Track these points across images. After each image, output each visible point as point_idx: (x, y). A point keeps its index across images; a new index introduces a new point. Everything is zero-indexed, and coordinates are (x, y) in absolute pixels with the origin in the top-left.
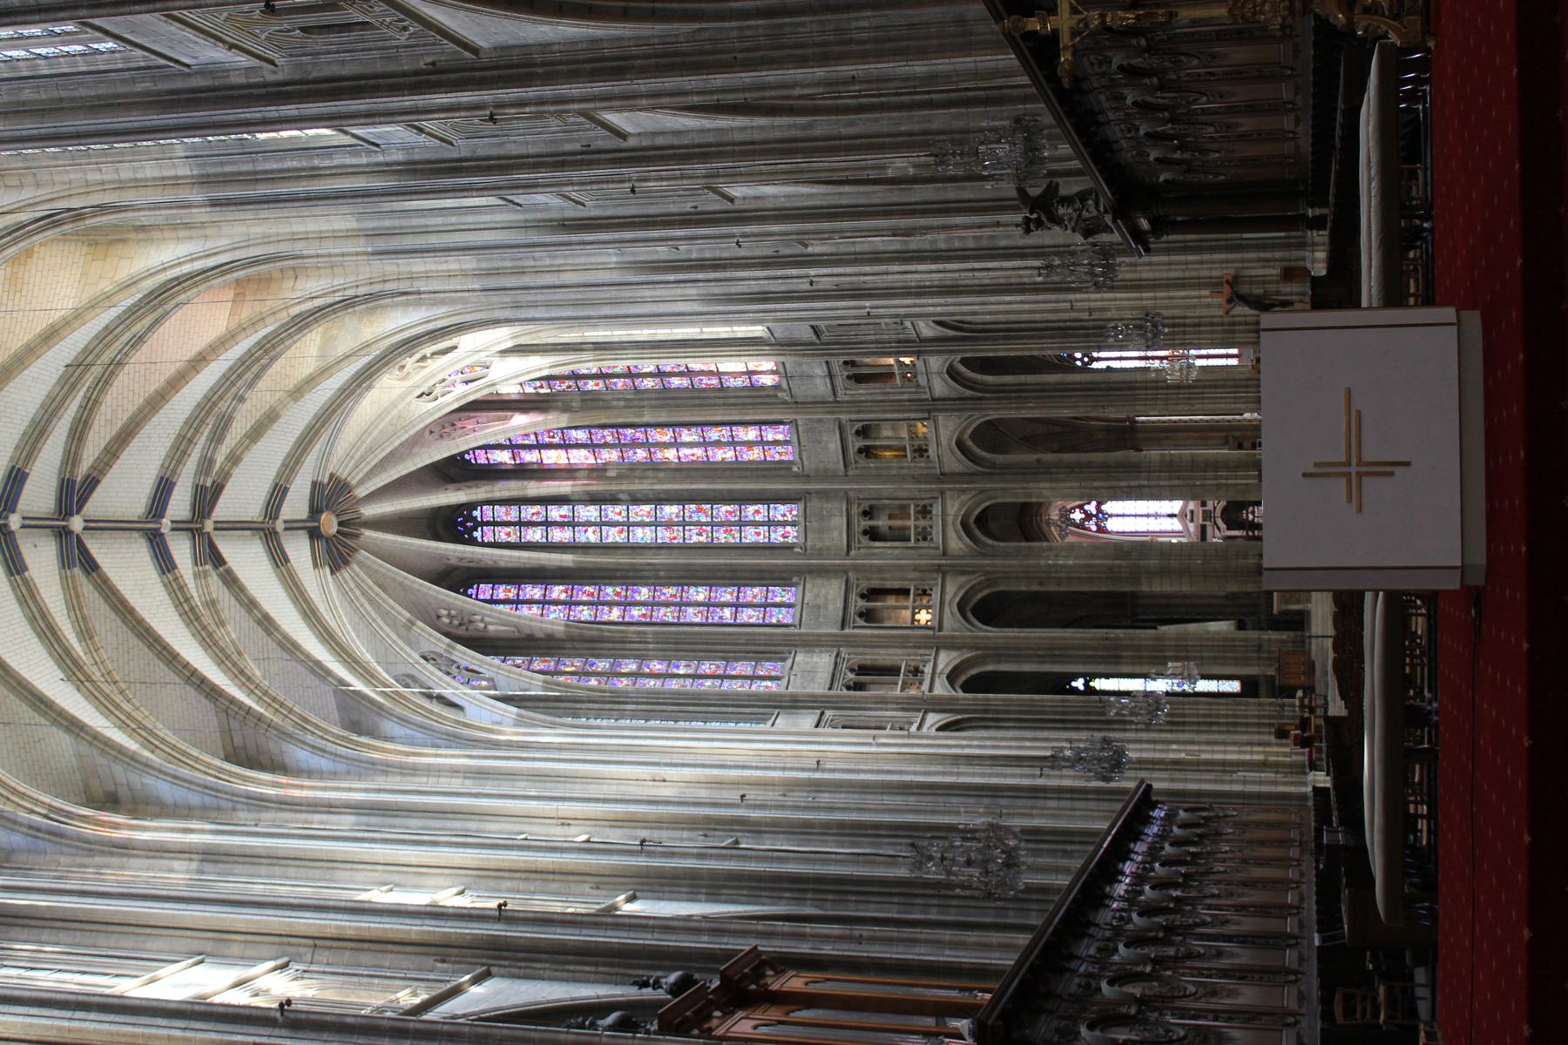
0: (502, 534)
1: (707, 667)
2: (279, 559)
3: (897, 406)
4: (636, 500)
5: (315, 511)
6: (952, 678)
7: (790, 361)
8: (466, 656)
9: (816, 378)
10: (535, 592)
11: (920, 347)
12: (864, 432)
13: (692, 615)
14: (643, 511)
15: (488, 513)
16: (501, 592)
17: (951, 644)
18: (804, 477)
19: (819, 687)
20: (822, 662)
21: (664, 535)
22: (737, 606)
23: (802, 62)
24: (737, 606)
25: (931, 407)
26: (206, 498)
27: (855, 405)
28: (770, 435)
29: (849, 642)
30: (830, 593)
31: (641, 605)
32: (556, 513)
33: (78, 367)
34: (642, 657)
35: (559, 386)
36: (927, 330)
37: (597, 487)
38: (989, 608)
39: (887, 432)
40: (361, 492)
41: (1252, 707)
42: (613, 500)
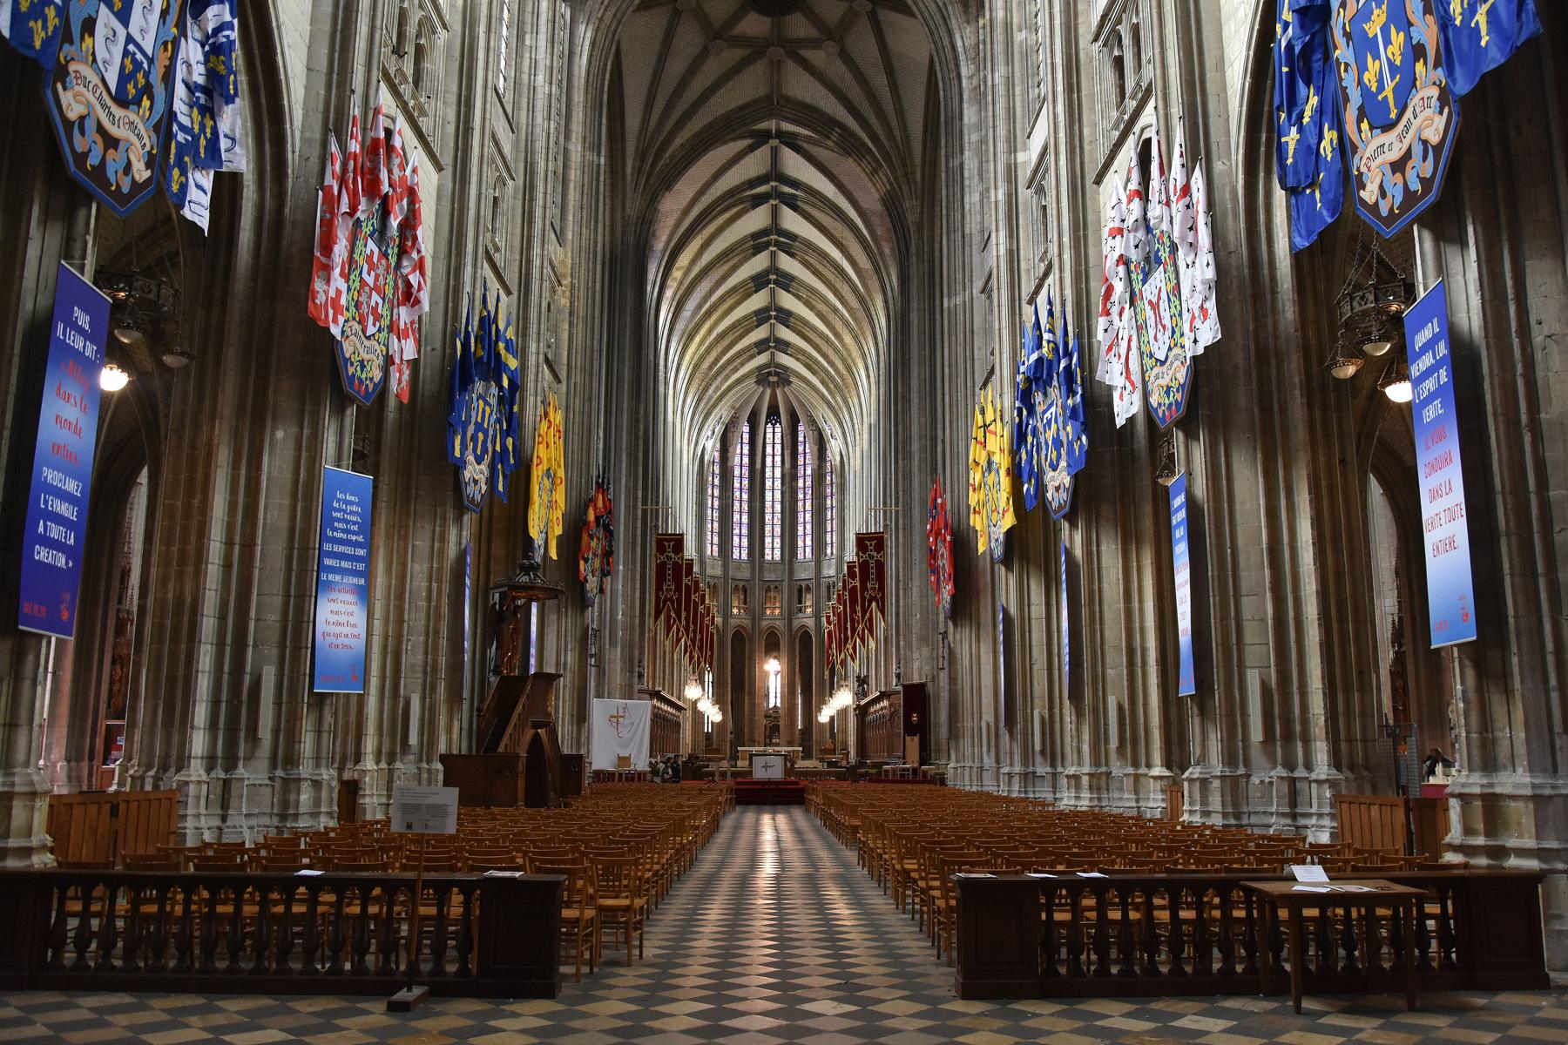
0: (769, 436)
1: (716, 525)
2: (759, 368)
4: (782, 493)
5: (777, 374)
8: (719, 430)
9: (829, 570)
12: (808, 588)
13: (736, 517)
14: (778, 495)
15: (778, 430)
16: (746, 437)
18: (791, 564)
19: (709, 571)
20: (718, 572)
21: (768, 504)
27: (818, 585)
28: (808, 550)
29: (726, 582)
30: (746, 574)
31: (741, 497)
32: (778, 459)
34: (720, 498)
38: (740, 638)
39: (809, 596)
41: (702, 739)
42: (783, 484)
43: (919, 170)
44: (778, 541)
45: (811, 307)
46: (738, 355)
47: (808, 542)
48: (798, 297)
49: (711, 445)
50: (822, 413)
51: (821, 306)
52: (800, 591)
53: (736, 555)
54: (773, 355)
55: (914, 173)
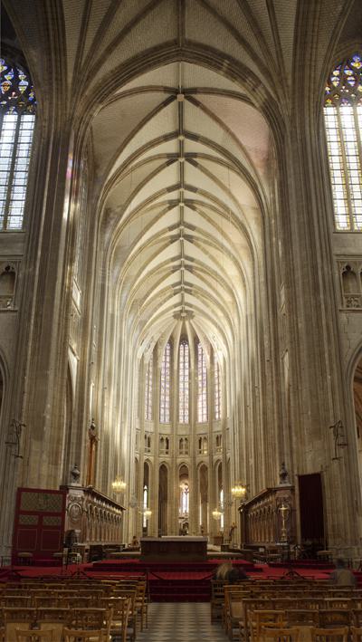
0: (182, 352)
1: (150, 402)
2: (175, 306)
3: (211, 448)
4: (190, 384)
5: (187, 311)
6: (147, 459)
7: (221, 422)
9: (218, 428)
10: (168, 359)
11: (225, 453)
13: (163, 397)
16: (168, 352)
17: (155, 460)
18: (195, 424)
21: (181, 390)
22: (164, 408)
23: (265, 449)
24: (164, 408)
25: (211, 455)
26: (189, 292)
27: (211, 438)
28: (205, 417)
29: (156, 435)
30: (167, 431)
32: (187, 364)
33: (216, 274)
35: (216, 366)
36: (228, 455)
37: (193, 375)
39: (205, 444)
40: (191, 321)
42: (190, 378)
43: (290, 77)
44: (187, 412)
45: (206, 253)
46: (162, 292)
47: (205, 412)
48: (198, 246)
49: (149, 355)
50: (212, 333)
51: (212, 251)
52: (200, 441)
53: (162, 420)
54: (183, 297)
55: (286, 79)
